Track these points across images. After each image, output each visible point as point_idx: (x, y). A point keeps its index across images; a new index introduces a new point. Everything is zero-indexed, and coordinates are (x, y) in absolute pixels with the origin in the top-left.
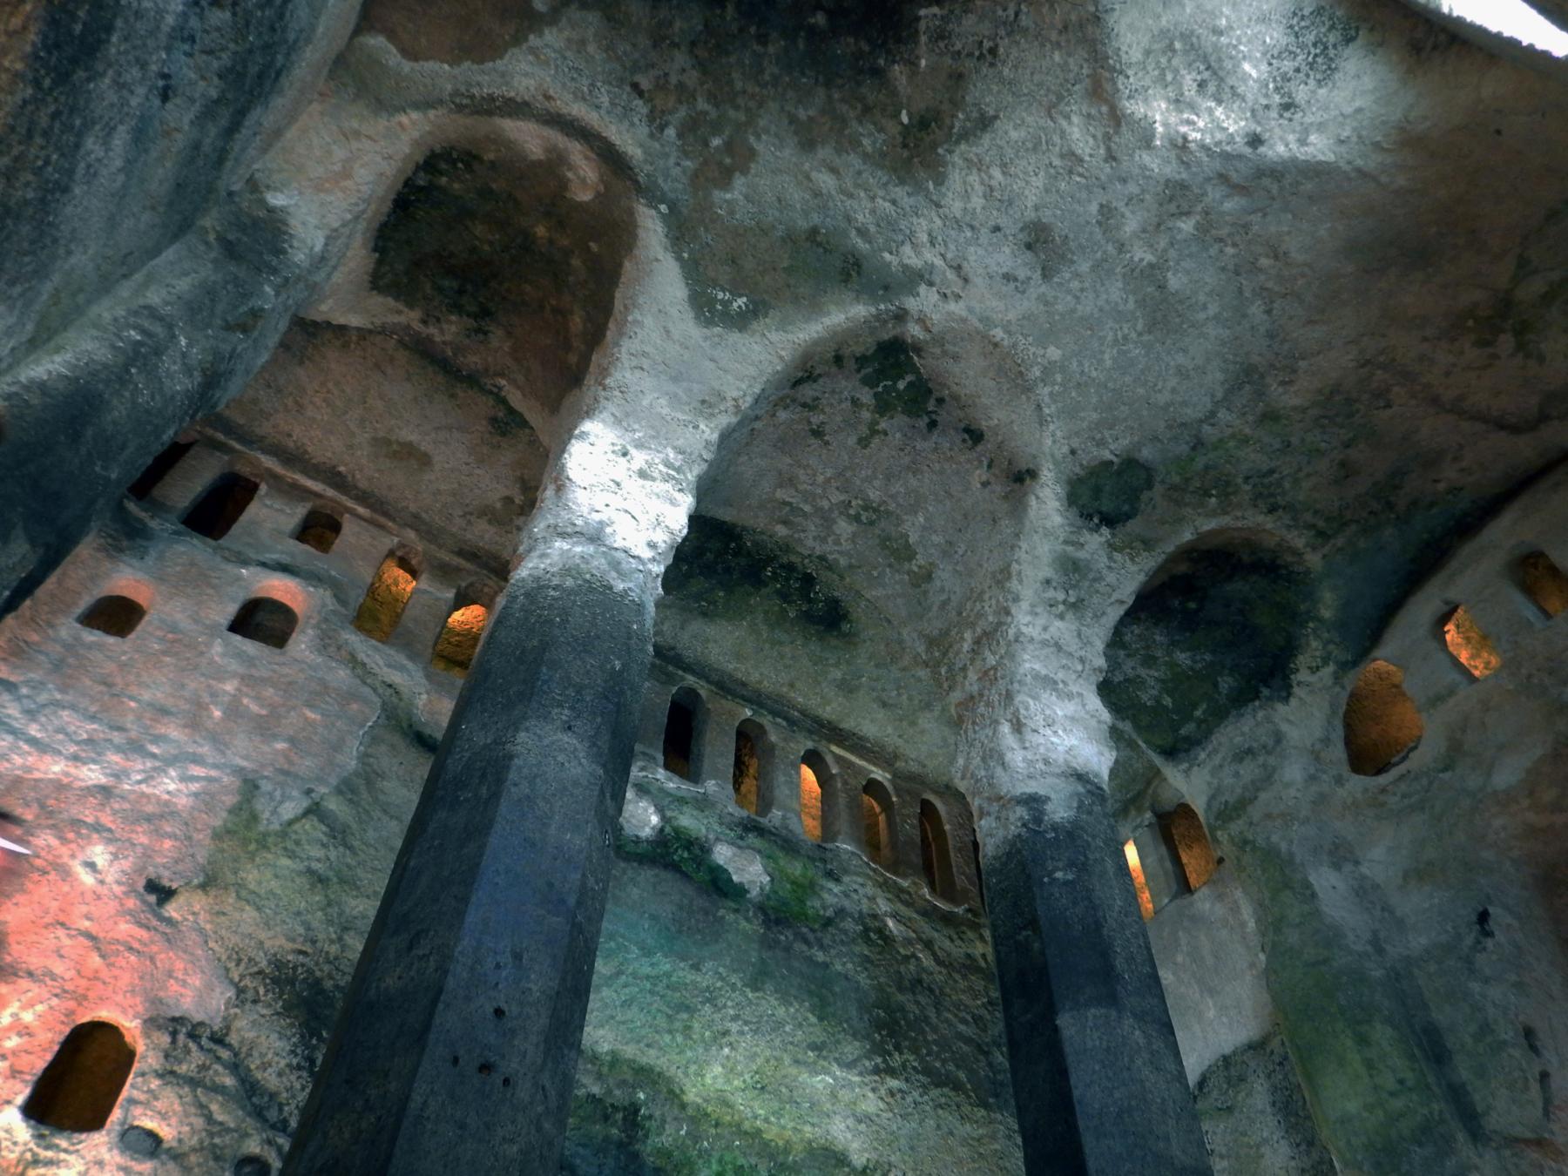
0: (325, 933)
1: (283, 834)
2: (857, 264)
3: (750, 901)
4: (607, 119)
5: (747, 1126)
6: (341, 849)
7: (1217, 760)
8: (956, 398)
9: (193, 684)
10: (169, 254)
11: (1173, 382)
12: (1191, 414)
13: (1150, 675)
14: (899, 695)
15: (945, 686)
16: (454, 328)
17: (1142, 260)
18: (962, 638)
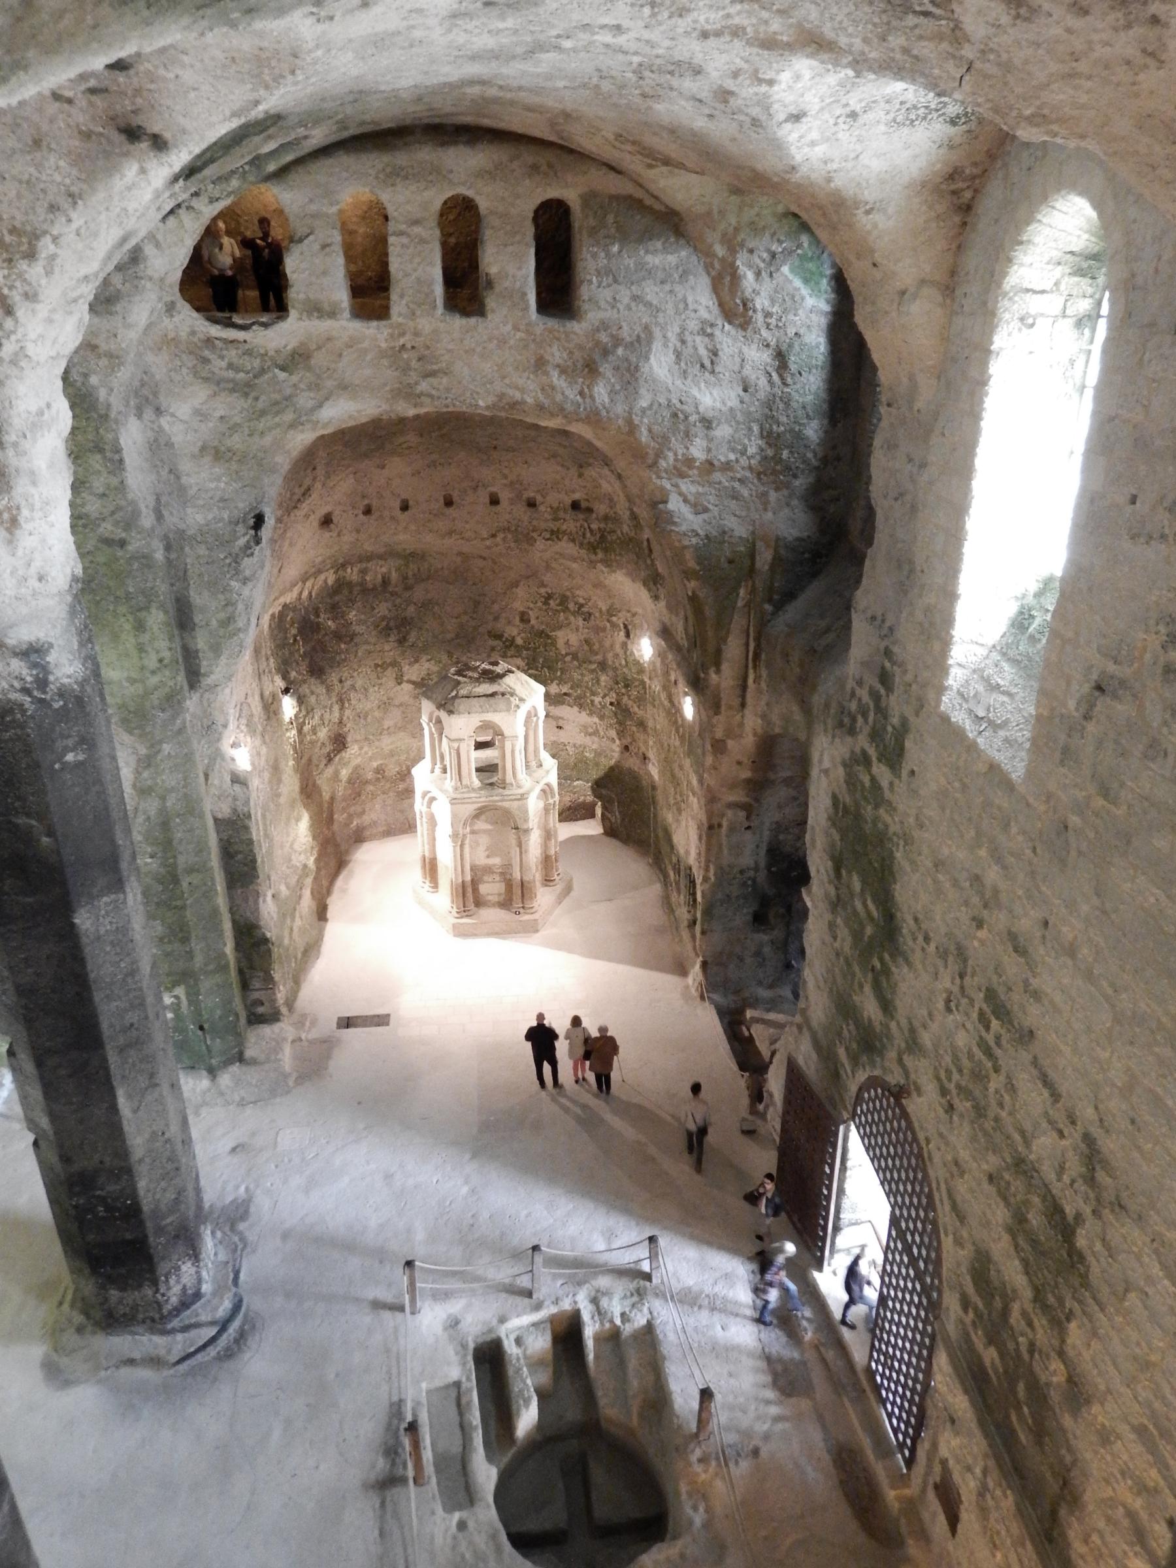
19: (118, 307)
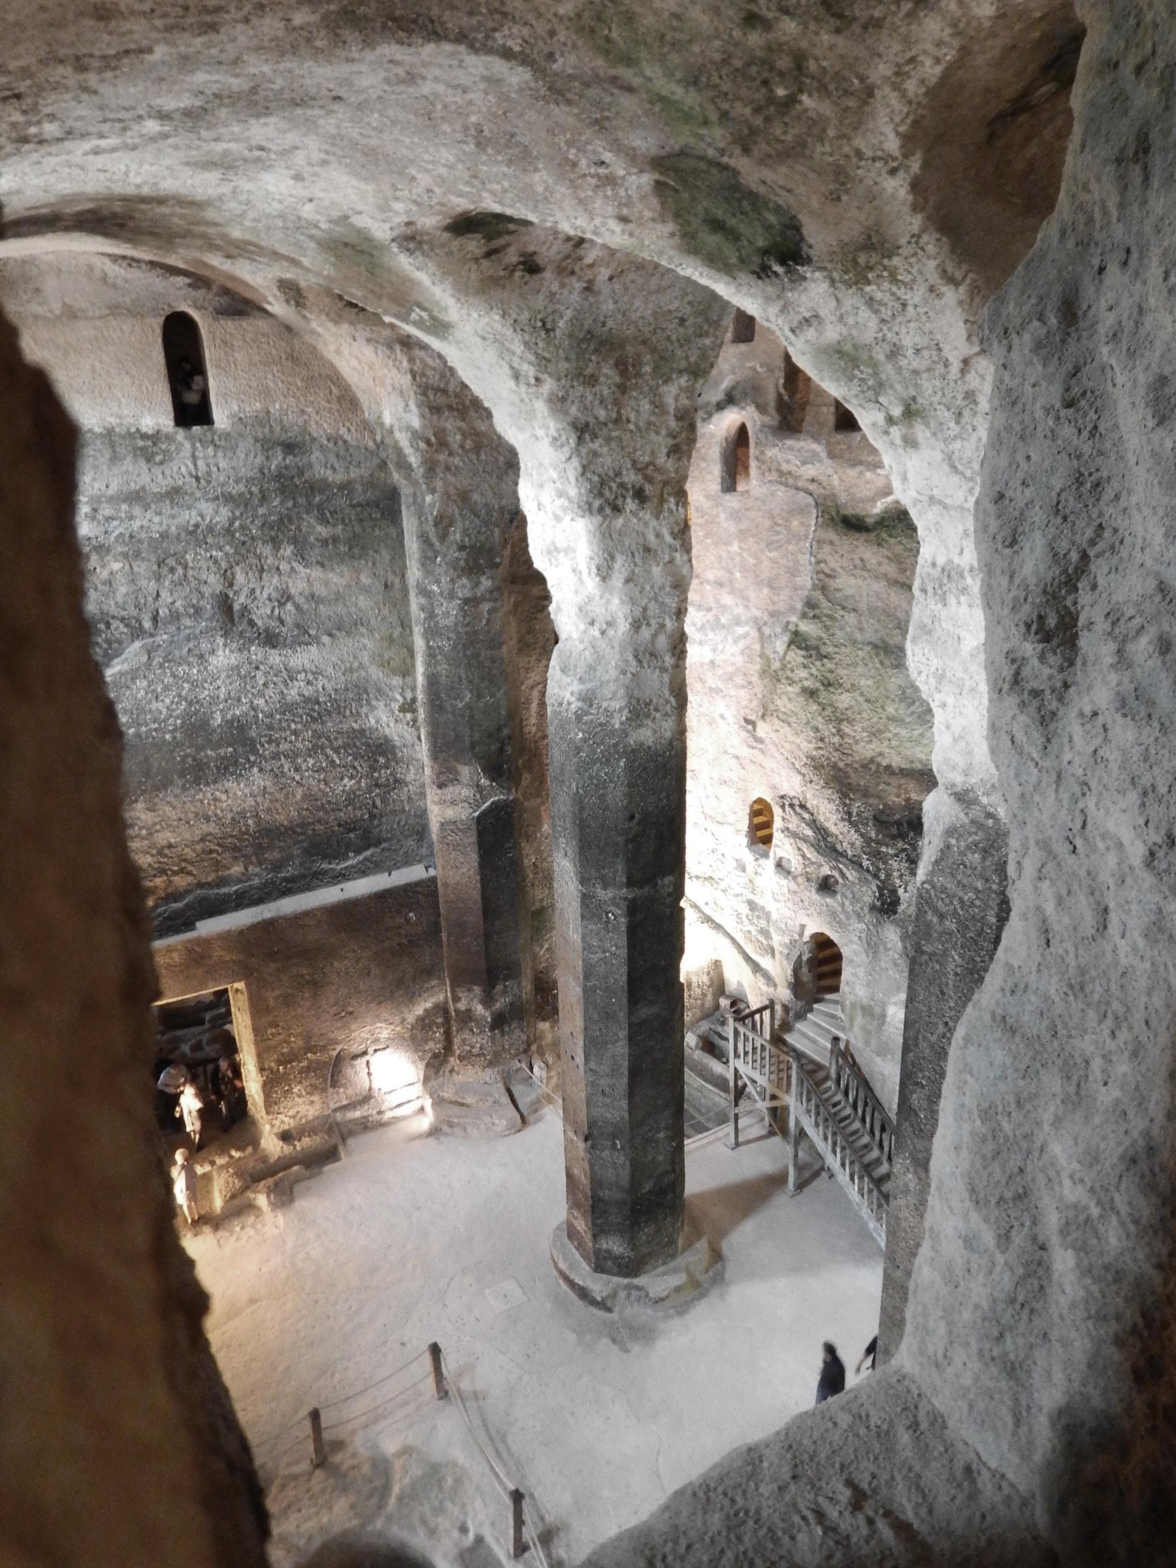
6: (818, 663)
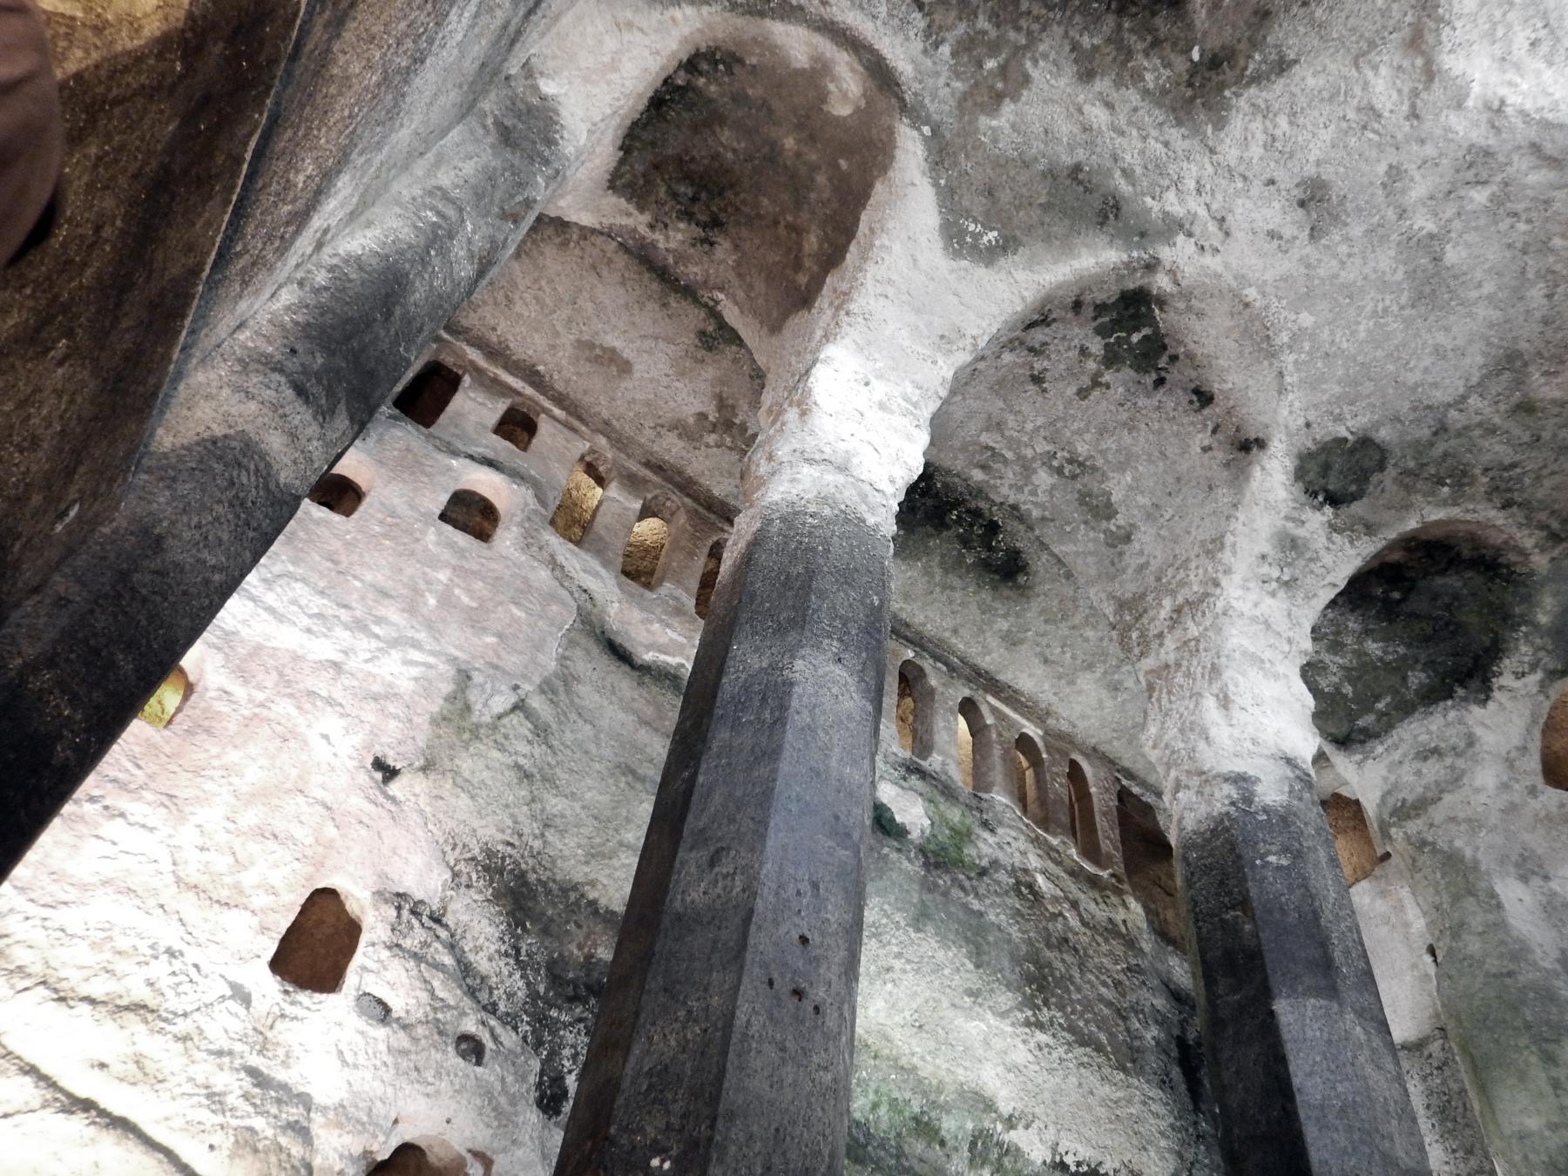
0: (530, 827)
1: (494, 727)
2: (1117, 208)
3: (912, 842)
4: (882, 29)
5: (903, 1061)
7: (1397, 756)
8: (1190, 356)
9: (410, 569)
10: (455, 134)
11: (1427, 362)
12: (1440, 396)
13: (1334, 662)
14: (1063, 652)
15: (1136, 651)
16: (680, 236)
17: (1422, 229)
18: (1160, 605)
19: (1465, 780)
